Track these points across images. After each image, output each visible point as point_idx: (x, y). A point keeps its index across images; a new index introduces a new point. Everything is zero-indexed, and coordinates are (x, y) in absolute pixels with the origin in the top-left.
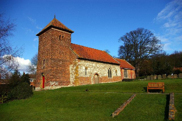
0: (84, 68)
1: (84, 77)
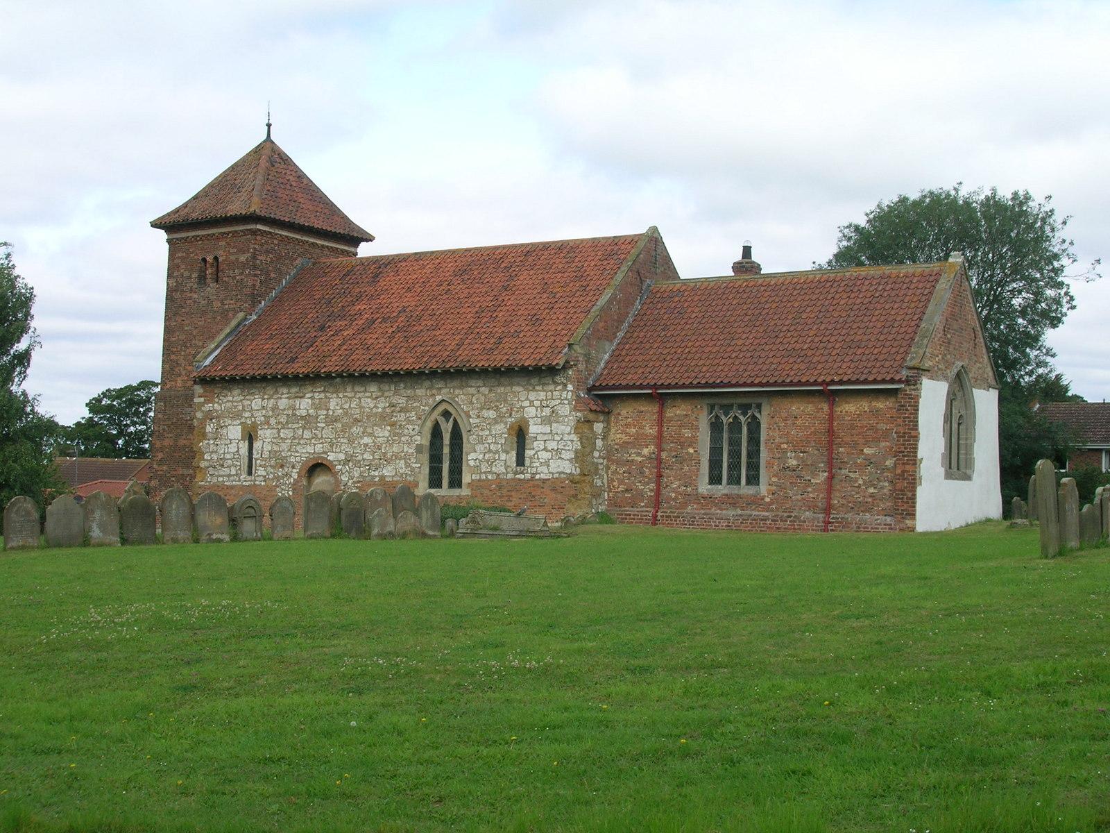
0: (235, 432)
1: (232, 487)
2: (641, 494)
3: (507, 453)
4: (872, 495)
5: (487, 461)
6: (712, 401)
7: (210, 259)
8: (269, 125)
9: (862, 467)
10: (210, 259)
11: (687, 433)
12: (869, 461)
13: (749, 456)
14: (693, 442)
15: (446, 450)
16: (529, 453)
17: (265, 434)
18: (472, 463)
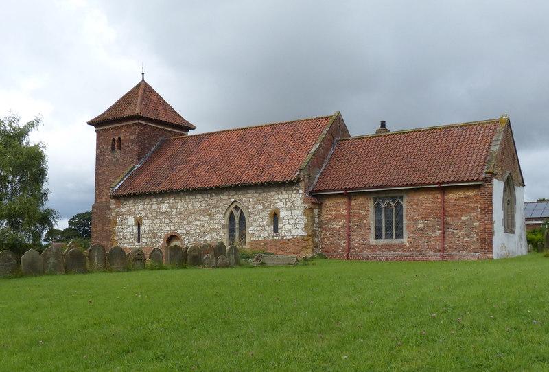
0: (131, 221)
2: (339, 245)
3: (269, 226)
4: (467, 242)
5: (259, 231)
6: (376, 196)
7: (116, 139)
8: (143, 74)
9: (460, 227)
10: (116, 139)
11: (363, 213)
12: (464, 224)
13: (397, 224)
14: (366, 217)
15: (237, 226)
16: (280, 226)
17: (146, 222)
18: (251, 232)
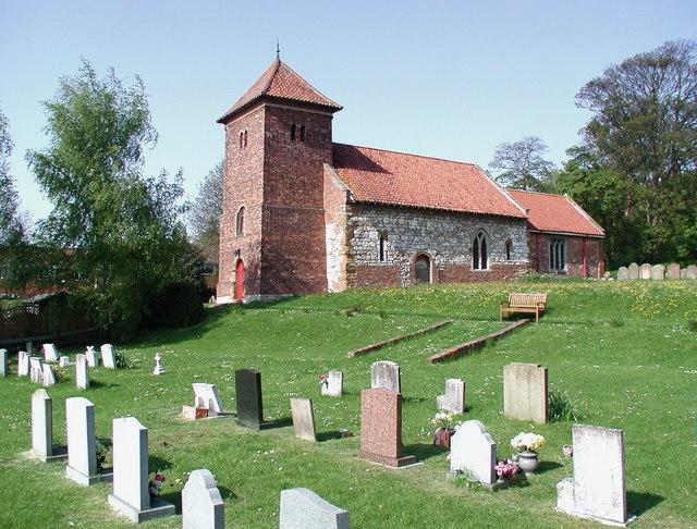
7: (299, 126)
10: (299, 126)
